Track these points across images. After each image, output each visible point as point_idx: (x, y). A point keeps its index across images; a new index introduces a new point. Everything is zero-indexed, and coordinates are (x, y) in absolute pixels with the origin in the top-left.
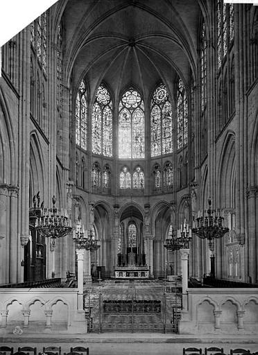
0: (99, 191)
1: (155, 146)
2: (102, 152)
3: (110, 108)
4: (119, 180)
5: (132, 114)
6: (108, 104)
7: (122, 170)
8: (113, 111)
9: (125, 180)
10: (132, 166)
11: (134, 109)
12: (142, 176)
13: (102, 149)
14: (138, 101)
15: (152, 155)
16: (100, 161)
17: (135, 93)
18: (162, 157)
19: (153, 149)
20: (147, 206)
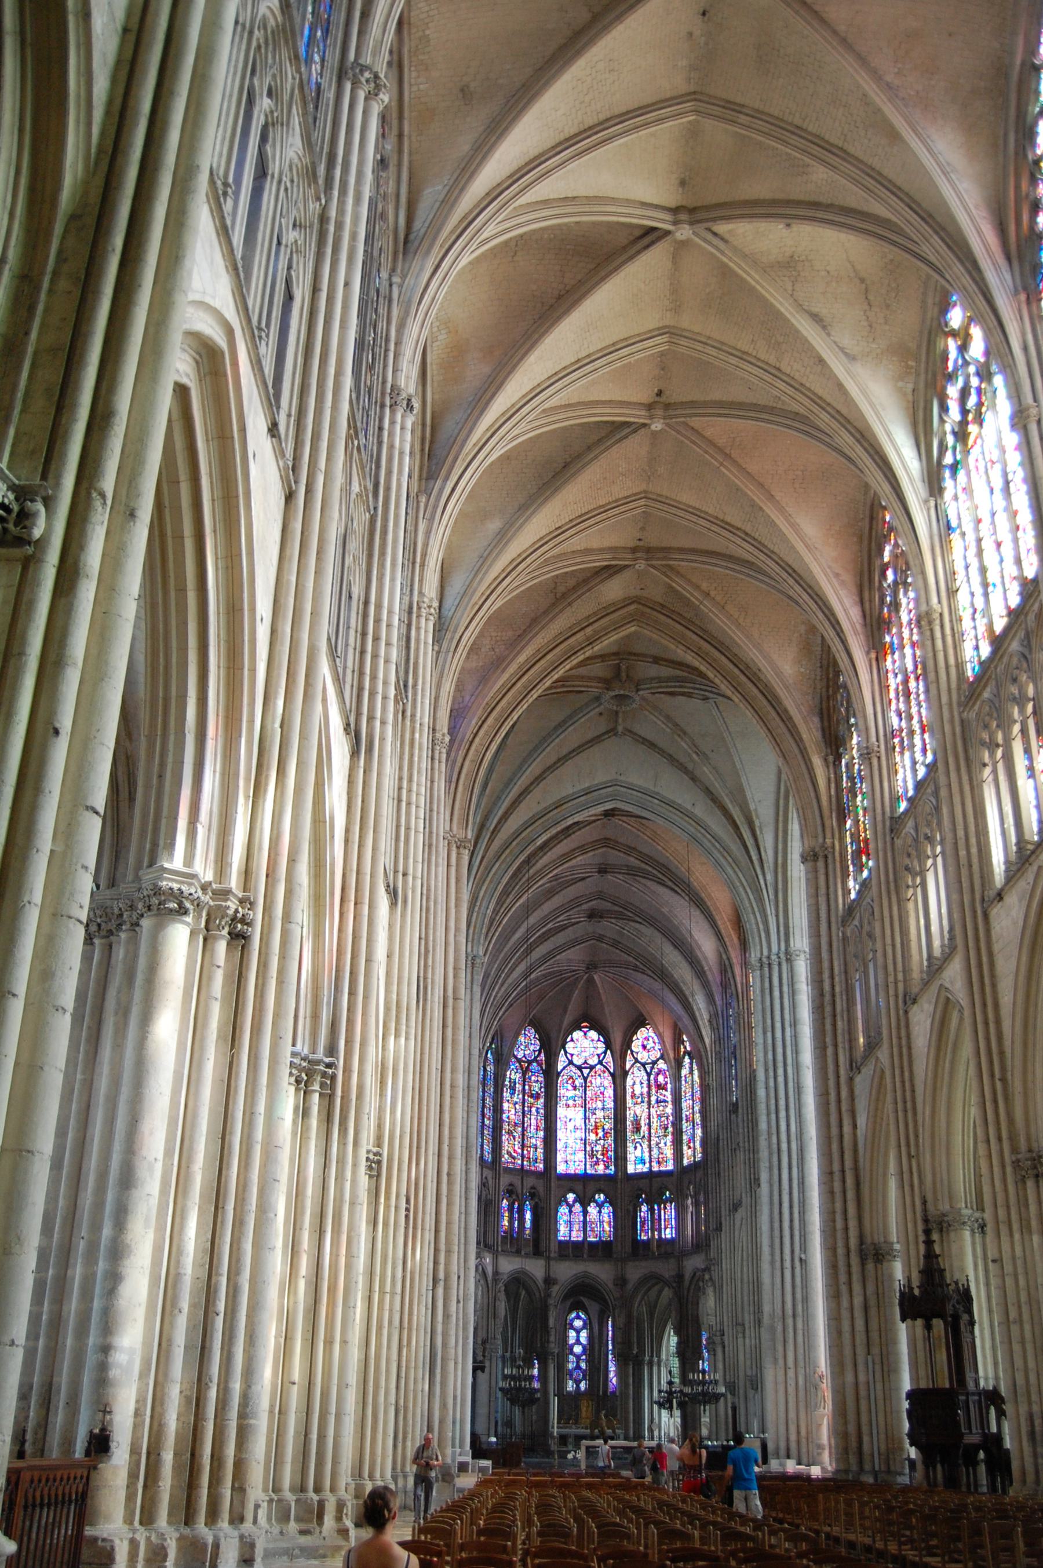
0: (513, 1243)
1: (636, 1148)
2: (523, 1161)
3: (540, 1064)
4: (556, 1222)
5: (585, 1079)
7: (562, 1200)
11: (592, 1068)
12: (607, 1210)
13: (523, 1156)
14: (600, 1051)
15: (631, 1169)
16: (517, 1182)
17: (593, 1034)
19: (631, 1157)
20: (621, 1281)
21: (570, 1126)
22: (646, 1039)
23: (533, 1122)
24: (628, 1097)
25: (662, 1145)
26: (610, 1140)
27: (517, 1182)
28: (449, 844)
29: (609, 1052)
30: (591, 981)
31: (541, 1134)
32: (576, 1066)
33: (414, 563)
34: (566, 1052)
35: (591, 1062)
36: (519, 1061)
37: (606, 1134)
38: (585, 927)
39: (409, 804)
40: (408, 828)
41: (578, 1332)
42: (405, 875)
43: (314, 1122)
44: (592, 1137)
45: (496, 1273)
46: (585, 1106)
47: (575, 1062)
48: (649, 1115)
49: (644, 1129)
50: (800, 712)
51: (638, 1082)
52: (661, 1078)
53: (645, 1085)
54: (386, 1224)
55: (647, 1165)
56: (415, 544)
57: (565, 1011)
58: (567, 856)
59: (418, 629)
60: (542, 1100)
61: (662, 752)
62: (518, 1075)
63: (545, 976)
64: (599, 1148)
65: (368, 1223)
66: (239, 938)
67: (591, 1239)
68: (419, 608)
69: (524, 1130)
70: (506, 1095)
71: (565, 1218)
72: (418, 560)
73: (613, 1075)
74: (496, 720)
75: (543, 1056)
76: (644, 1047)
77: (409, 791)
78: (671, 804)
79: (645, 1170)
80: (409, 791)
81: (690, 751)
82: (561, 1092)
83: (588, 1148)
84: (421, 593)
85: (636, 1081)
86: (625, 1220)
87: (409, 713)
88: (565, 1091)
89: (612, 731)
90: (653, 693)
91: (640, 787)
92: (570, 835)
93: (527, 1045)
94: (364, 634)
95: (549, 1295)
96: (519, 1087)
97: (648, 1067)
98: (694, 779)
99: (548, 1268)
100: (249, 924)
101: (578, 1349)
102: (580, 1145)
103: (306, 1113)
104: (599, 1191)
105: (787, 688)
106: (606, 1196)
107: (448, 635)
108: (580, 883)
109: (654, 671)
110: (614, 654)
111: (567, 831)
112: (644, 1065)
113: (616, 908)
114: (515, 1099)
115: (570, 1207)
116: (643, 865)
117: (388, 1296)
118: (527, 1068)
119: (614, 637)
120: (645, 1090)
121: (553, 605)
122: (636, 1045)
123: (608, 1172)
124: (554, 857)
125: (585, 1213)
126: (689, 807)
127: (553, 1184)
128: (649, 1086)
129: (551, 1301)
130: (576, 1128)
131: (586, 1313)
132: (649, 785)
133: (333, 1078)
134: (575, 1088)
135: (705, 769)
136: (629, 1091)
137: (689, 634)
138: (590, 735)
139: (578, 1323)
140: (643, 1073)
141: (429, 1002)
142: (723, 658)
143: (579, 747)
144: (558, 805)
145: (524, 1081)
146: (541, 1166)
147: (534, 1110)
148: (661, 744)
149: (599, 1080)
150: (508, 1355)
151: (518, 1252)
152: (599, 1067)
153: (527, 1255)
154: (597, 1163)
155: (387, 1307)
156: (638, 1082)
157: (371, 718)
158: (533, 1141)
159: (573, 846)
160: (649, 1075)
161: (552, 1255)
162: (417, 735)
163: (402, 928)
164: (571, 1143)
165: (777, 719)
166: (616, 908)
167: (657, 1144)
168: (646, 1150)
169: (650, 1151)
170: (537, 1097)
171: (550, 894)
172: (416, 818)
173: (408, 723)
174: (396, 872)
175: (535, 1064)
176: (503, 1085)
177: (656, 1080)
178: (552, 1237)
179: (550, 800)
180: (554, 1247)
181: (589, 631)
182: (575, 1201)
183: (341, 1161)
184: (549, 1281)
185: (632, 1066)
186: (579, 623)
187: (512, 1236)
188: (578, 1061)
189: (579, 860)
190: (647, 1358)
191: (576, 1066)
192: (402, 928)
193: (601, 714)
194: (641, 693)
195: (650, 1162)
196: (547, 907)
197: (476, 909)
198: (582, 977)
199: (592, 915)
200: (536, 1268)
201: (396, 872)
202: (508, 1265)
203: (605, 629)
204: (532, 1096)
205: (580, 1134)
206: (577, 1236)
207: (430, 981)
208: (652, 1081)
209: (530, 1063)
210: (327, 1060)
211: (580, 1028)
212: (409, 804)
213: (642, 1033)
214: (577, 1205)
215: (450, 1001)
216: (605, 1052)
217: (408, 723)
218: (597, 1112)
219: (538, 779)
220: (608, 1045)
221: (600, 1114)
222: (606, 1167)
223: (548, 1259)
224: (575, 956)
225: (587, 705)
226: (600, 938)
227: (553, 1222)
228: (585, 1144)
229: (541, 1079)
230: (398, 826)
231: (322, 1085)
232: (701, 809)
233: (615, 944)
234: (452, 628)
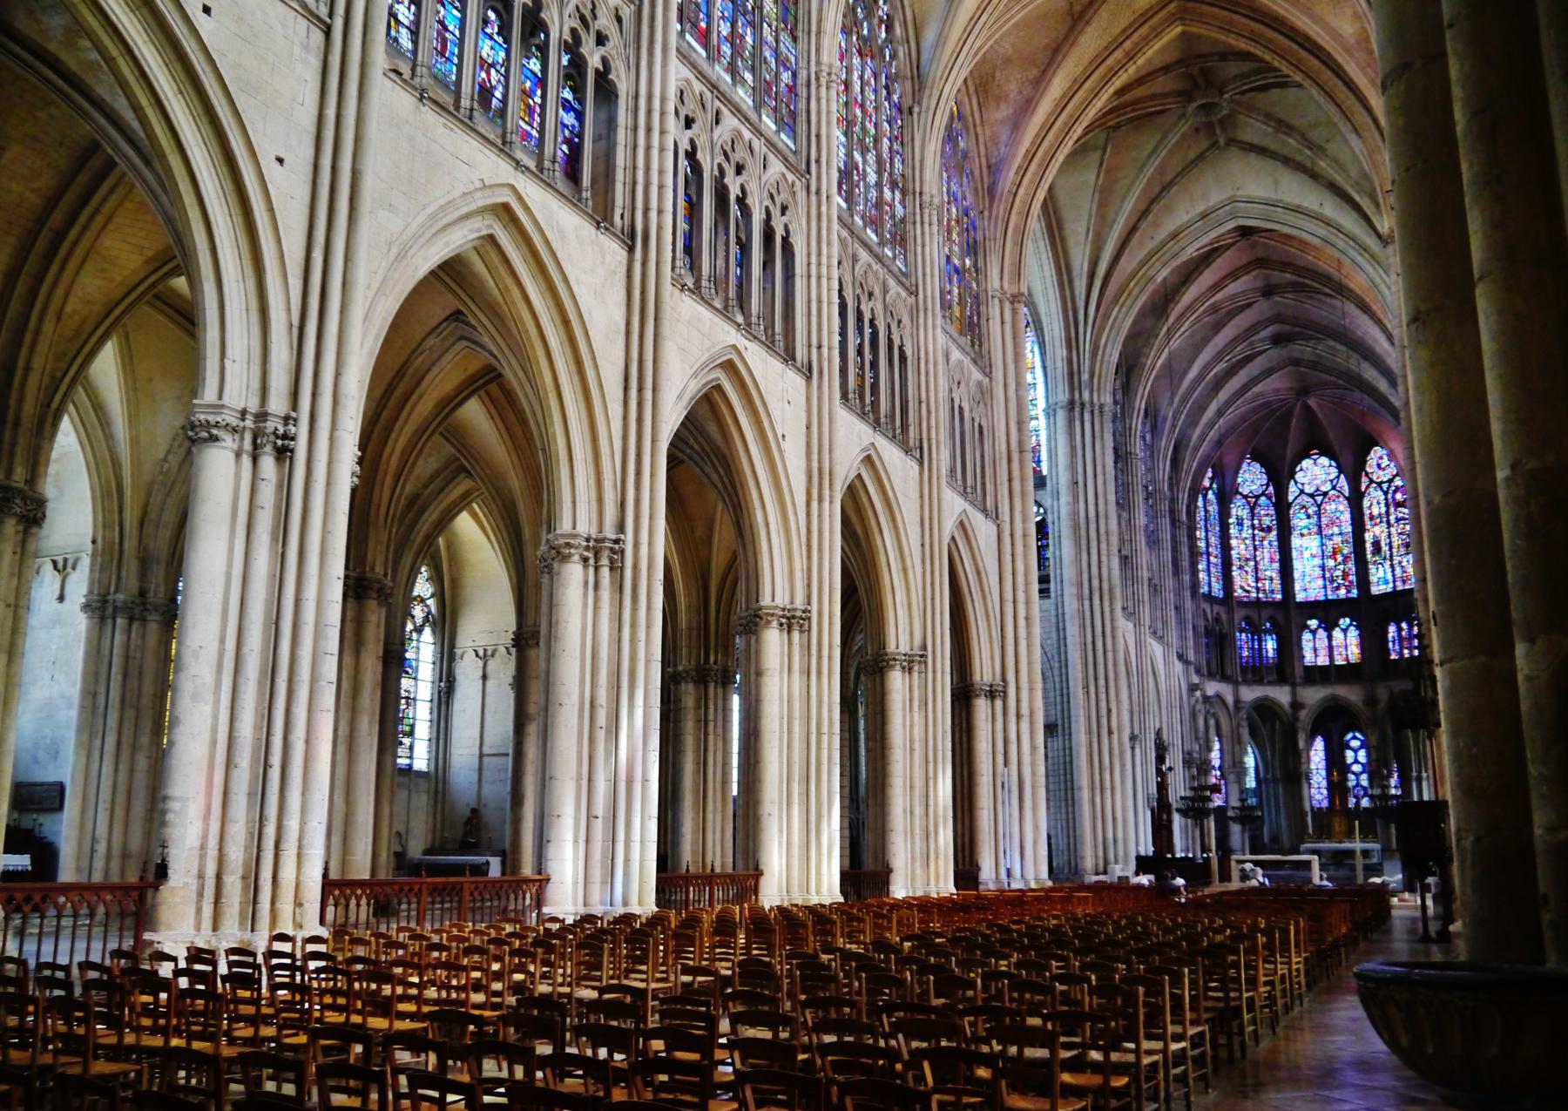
3: (1269, 498)
4: (1301, 649)
5: (1319, 506)
6: (1263, 494)
8: (1274, 505)
9: (1314, 649)
10: (1328, 612)
11: (1325, 494)
12: (1353, 633)
13: (1258, 589)
14: (1332, 477)
15: (1375, 590)
16: (1255, 616)
17: (1324, 461)
18: (1395, 592)
19: (1373, 579)
20: (1371, 701)
21: (1307, 554)
22: (1381, 458)
23: (1267, 555)
24: (1366, 518)
25: (1404, 564)
26: (1351, 565)
27: (1254, 614)
28: (1001, 301)
29: (1342, 476)
30: (1307, 408)
31: (1276, 565)
32: (1308, 495)
33: (809, 33)
34: (1296, 483)
35: (1324, 489)
36: (1245, 497)
37: (1345, 561)
38: (1274, 354)
39: (819, 278)
40: (820, 301)
41: (1355, 751)
42: (819, 347)
43: (606, 594)
44: (1331, 563)
45: (1237, 701)
46: (1320, 532)
47: (1307, 491)
48: (1389, 536)
49: (1385, 548)
50: (1365, 74)
51: (1375, 502)
52: (1399, 496)
53: (1383, 505)
54: (819, 673)
55: (1391, 585)
56: (809, 12)
57: (1286, 442)
58: (1218, 286)
59: (818, 100)
60: (1275, 533)
61: (1274, 155)
62: (1246, 511)
63: (1254, 410)
64: (1338, 573)
65: (801, 673)
66: (284, 453)
67: (1339, 661)
68: (817, 79)
69: (1257, 563)
70: (1233, 531)
71: (1311, 644)
72: (814, 28)
73: (1347, 498)
74: (1040, 165)
75: (1271, 489)
76: (1379, 466)
77: (819, 265)
78: (1297, 210)
79: (1389, 590)
80: (819, 265)
81: (1300, 147)
82: (1294, 522)
83: (1328, 575)
84: (818, 63)
85: (1374, 502)
86: (1373, 641)
87: (813, 188)
88: (1299, 521)
89: (1215, 144)
90: (1243, 93)
91: (1261, 198)
92: (1210, 264)
93: (1252, 478)
94: (635, 129)
95: (1295, 719)
96: (1247, 523)
97: (1385, 486)
98: (1315, 176)
99: (1294, 694)
100: (293, 439)
101: (1356, 768)
102: (1318, 572)
103: (597, 586)
104: (1344, 616)
105: (1347, 50)
106: (1320, 622)
107: (927, 92)
108: (1248, 312)
109: (1233, 69)
110: (1180, 62)
111: (1206, 259)
112: (1380, 484)
113: (1297, 329)
114: (1244, 535)
115: (1314, 632)
116: (1301, 280)
117: (825, 738)
118: (1255, 503)
119: (1158, 45)
120: (1383, 510)
121: (1072, 29)
122: (1371, 466)
123: (1350, 595)
124: (1204, 289)
125: (1330, 638)
126: (1316, 208)
127: (1293, 613)
128: (1387, 505)
129: (1299, 725)
130: (1313, 556)
131: (1363, 734)
132: (1270, 194)
133: (622, 552)
134: (1309, 517)
135: (1322, 164)
136: (1367, 512)
137: (1236, 17)
138: (1192, 155)
139: (1355, 744)
140: (1380, 493)
141: (934, 462)
142: (1280, 38)
143: (1184, 169)
144: (1174, 236)
145: (1253, 515)
146: (1279, 597)
147: (1266, 543)
148: (1274, 147)
149: (1333, 506)
150: (1269, 776)
151: (1260, 682)
152: (1333, 492)
153: (1270, 683)
154: (1338, 588)
155: (825, 744)
156: (1375, 502)
157: (646, 210)
158: (1268, 573)
159: (1223, 273)
160: (1386, 493)
161: (1298, 681)
162: (824, 208)
163: (820, 399)
164: (1308, 572)
165: (1345, 89)
166: (1297, 329)
167: (1400, 563)
168: (1389, 570)
169: (1393, 570)
170: (1269, 530)
171: (1217, 328)
172: (829, 290)
173: (813, 198)
174: (810, 346)
175: (1263, 498)
176: (1229, 524)
177: (1393, 497)
178: (1296, 663)
179: (1163, 234)
180: (1299, 672)
181: (1127, 45)
182: (1319, 627)
183: (633, 625)
184: (1296, 705)
185: (1368, 487)
186: (1115, 39)
187: (1254, 666)
188: (1308, 489)
189: (1233, 288)
190: (1414, 774)
191: (1308, 495)
192: (820, 399)
193: (1197, 130)
194: (1226, 96)
195: (1394, 581)
196: (1220, 340)
197: (1099, 358)
198: (1295, 405)
199: (1277, 340)
200: (1282, 695)
201: (810, 346)
202: (1250, 694)
203: (1147, 36)
204: (1262, 530)
205: (1317, 561)
206: (1323, 660)
207: (934, 441)
208: (1390, 501)
209: (1257, 497)
210: (613, 537)
211: (1308, 456)
212: (819, 278)
213: (1377, 452)
214: (1321, 631)
215: (1015, 456)
216: (1338, 477)
217: (813, 198)
218: (1335, 538)
219: (1145, 213)
220: (1340, 473)
221: (1338, 539)
222: (1348, 592)
223: (1294, 685)
224: (1276, 384)
225: (1175, 124)
226: (1296, 362)
227: (1295, 648)
228: (1323, 570)
229: (1272, 512)
230: (809, 301)
231: (612, 561)
232: (1330, 208)
233: (1315, 365)
234: (929, 84)
